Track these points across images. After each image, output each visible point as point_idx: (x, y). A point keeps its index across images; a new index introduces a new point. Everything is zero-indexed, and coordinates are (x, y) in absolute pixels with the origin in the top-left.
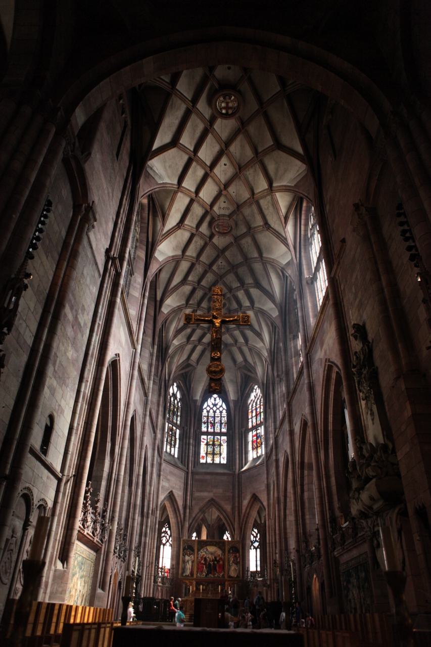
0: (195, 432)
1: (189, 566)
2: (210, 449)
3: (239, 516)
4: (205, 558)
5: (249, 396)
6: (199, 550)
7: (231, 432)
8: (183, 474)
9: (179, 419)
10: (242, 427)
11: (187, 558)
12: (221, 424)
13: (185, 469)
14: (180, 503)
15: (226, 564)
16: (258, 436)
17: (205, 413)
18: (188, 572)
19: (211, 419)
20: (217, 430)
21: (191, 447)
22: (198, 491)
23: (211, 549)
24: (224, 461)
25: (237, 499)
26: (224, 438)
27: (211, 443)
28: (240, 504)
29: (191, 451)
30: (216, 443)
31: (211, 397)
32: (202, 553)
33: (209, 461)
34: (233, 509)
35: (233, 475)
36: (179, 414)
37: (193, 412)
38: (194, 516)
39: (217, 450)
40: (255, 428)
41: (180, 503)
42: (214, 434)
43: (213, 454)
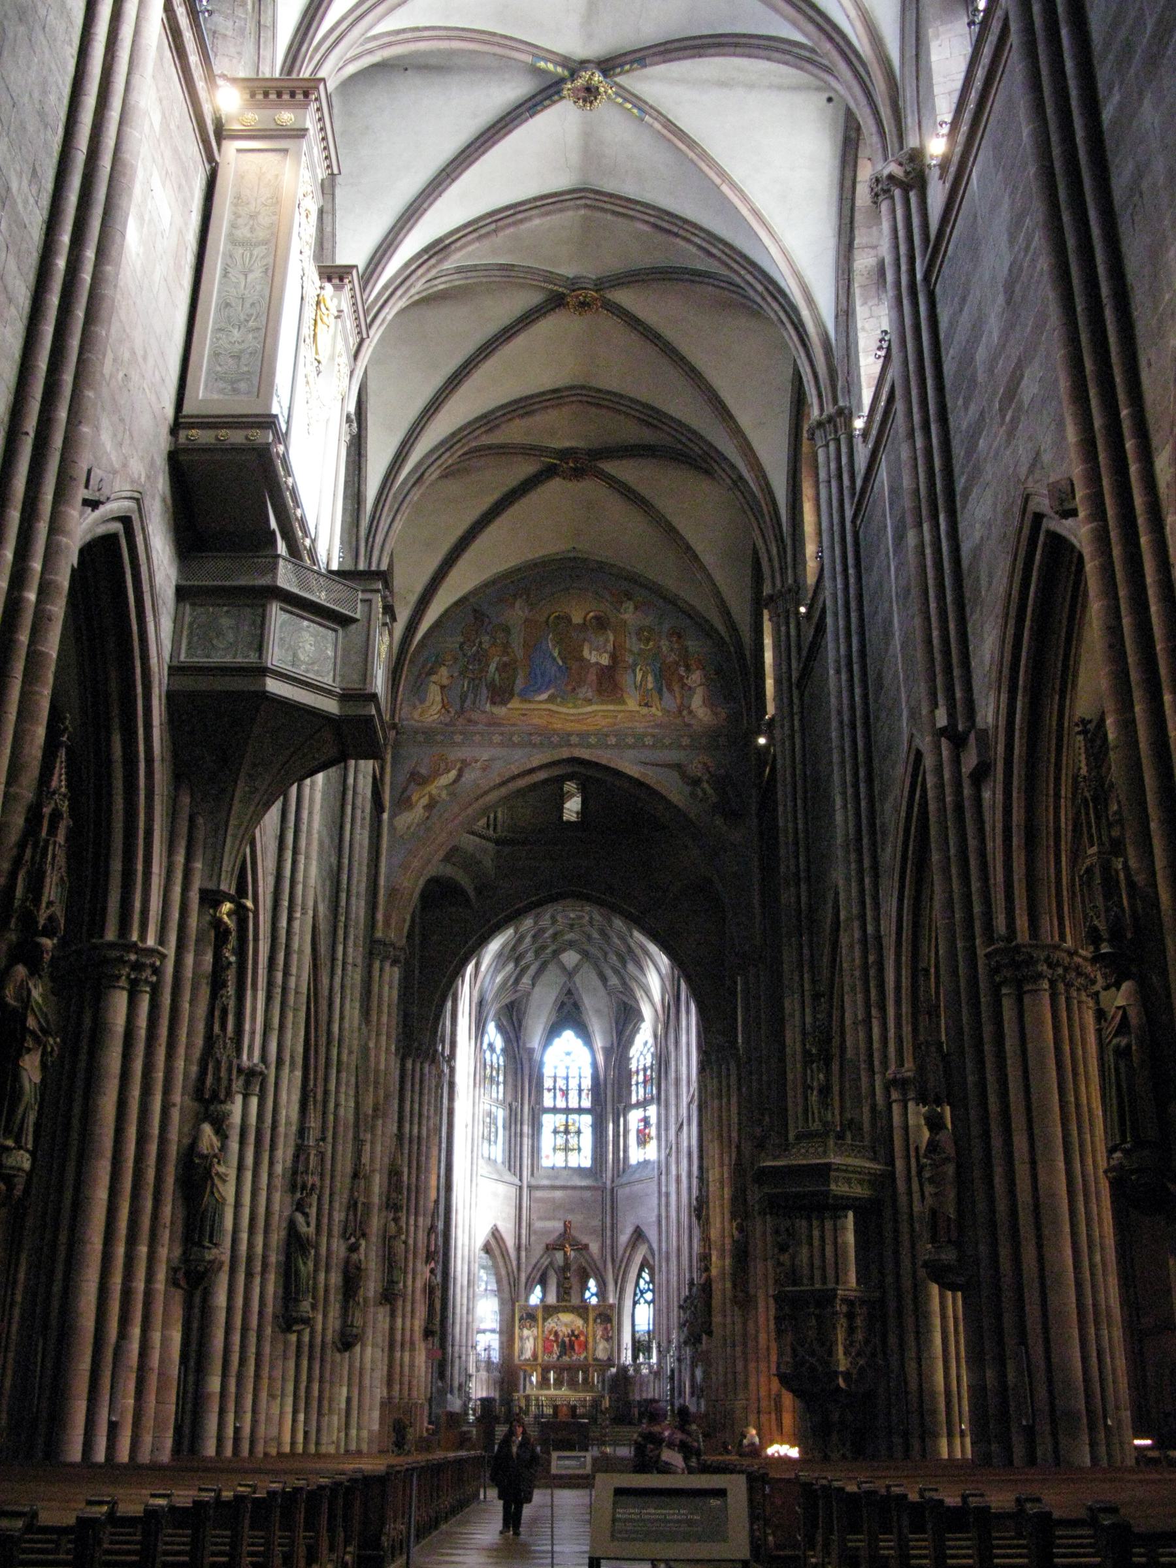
0: (532, 1110)
1: (529, 1345)
2: (560, 1140)
3: (613, 1260)
4: (556, 1334)
5: (630, 1042)
6: (545, 1320)
7: (598, 1109)
8: (513, 1191)
9: (501, 1087)
10: (620, 1102)
11: (526, 1332)
12: (580, 1091)
13: (517, 1181)
14: (510, 1242)
15: (590, 1340)
16: (646, 1121)
17: (548, 1071)
18: (528, 1354)
19: (561, 1083)
20: (573, 1104)
21: (525, 1140)
22: (540, 1219)
23: (566, 1318)
24: (587, 1163)
25: (609, 1234)
26: (587, 1120)
27: (562, 1129)
28: (613, 1238)
29: (525, 1148)
30: (572, 1129)
31: (559, 1035)
32: (551, 1324)
33: (560, 1163)
34: (603, 1247)
35: (603, 1189)
36: (501, 1079)
37: (526, 1072)
38: (533, 1261)
39: (573, 1141)
40: (643, 1104)
41: (510, 1242)
42: (567, 1111)
43: (566, 1149)
